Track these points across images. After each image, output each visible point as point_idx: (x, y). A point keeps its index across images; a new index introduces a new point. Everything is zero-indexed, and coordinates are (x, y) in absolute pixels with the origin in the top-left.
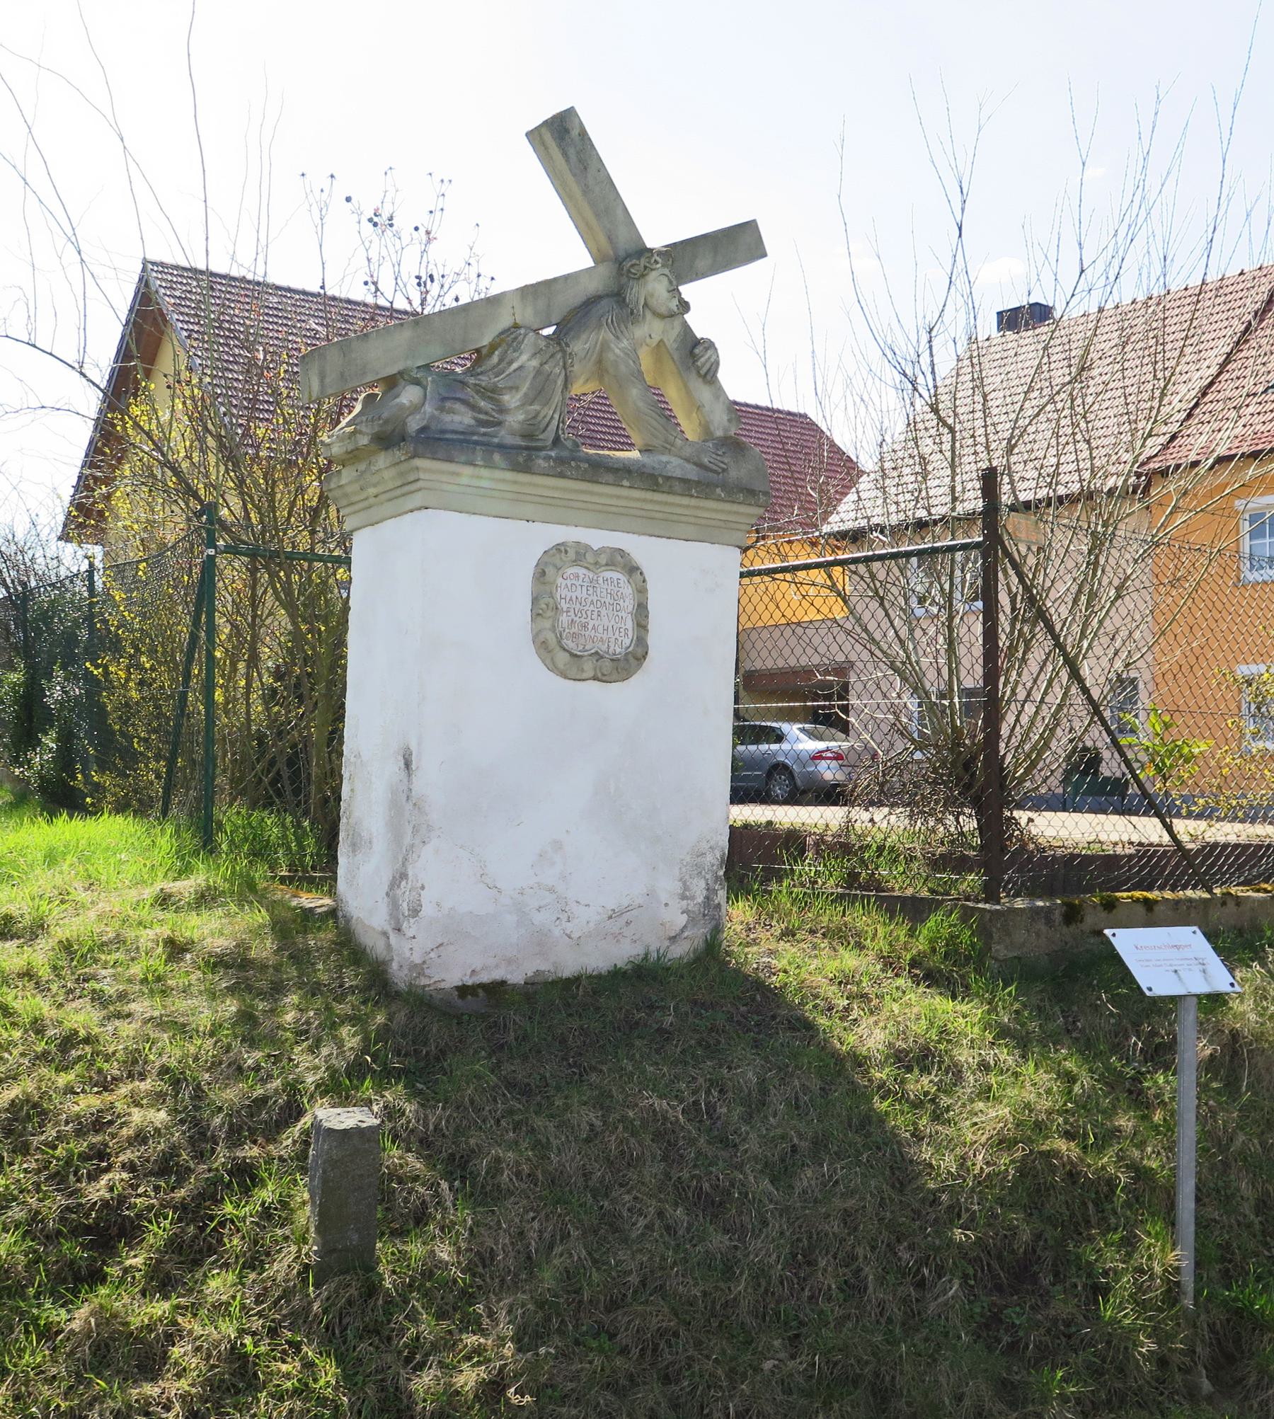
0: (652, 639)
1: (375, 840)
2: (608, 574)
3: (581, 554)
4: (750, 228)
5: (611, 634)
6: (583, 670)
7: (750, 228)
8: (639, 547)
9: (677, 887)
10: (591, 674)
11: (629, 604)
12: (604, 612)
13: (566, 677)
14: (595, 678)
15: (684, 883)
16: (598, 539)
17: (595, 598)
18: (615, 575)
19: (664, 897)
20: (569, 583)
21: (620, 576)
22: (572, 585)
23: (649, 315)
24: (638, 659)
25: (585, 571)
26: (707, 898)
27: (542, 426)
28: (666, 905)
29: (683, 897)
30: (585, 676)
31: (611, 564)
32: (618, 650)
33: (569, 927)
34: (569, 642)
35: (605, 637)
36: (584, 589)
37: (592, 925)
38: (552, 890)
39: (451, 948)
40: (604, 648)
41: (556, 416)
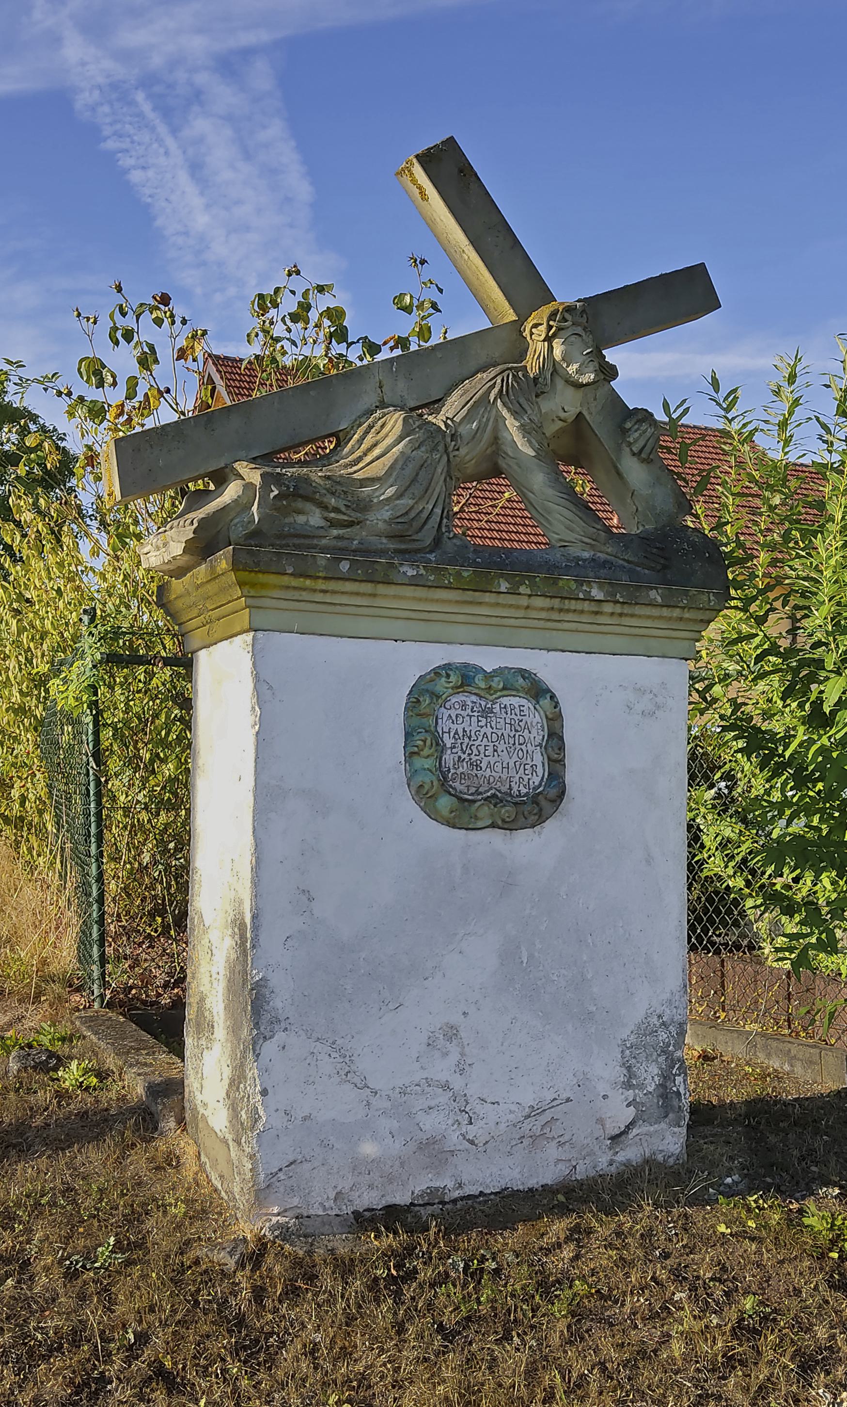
0: (571, 777)
1: (215, 1024)
2: (506, 701)
3: (466, 677)
4: (696, 277)
5: (512, 773)
6: (476, 818)
7: (696, 277)
8: (545, 665)
9: (618, 1073)
10: (489, 822)
11: (537, 735)
12: (501, 747)
13: (454, 827)
14: (493, 826)
15: (629, 1068)
16: (489, 659)
17: (489, 731)
18: (515, 701)
19: (602, 1088)
20: (453, 713)
21: (523, 702)
22: (455, 718)
23: (560, 383)
24: (553, 801)
25: (474, 698)
26: (662, 1086)
27: (416, 525)
28: (605, 1097)
29: (628, 1085)
30: (480, 824)
31: (508, 688)
32: (524, 791)
33: (472, 1131)
34: (456, 784)
35: (504, 777)
36: (474, 719)
37: (503, 1126)
38: (446, 1087)
39: (307, 1166)
40: (504, 789)
41: (438, 511)
